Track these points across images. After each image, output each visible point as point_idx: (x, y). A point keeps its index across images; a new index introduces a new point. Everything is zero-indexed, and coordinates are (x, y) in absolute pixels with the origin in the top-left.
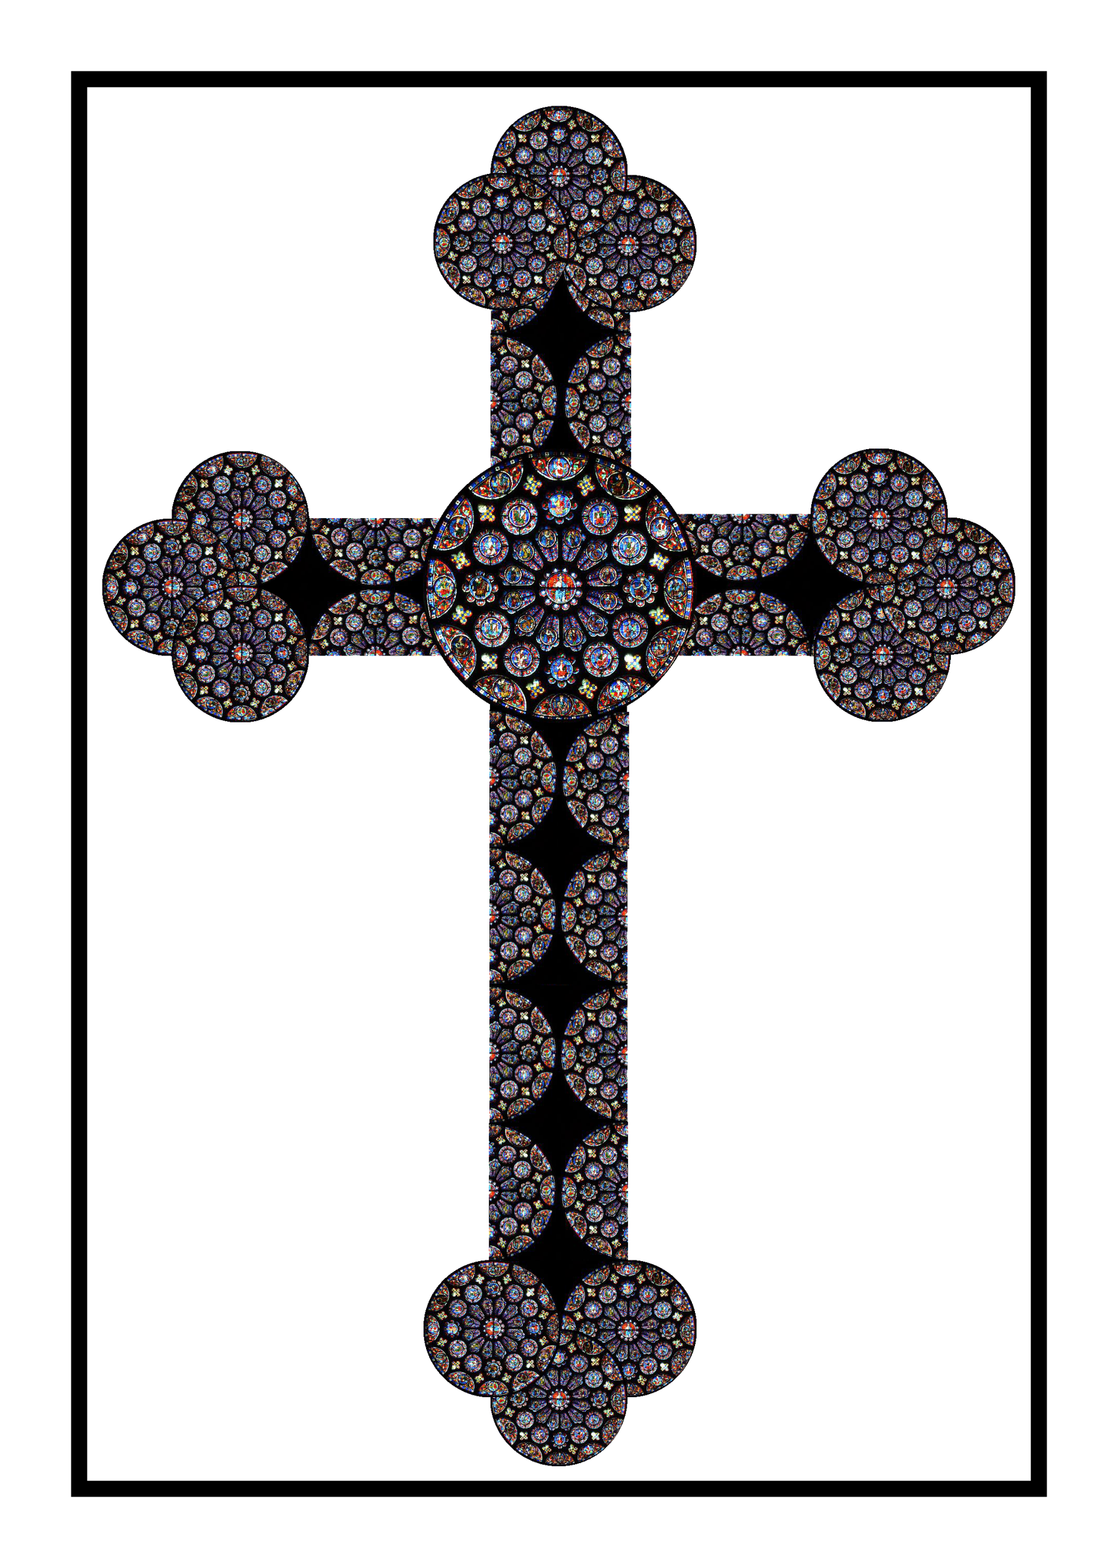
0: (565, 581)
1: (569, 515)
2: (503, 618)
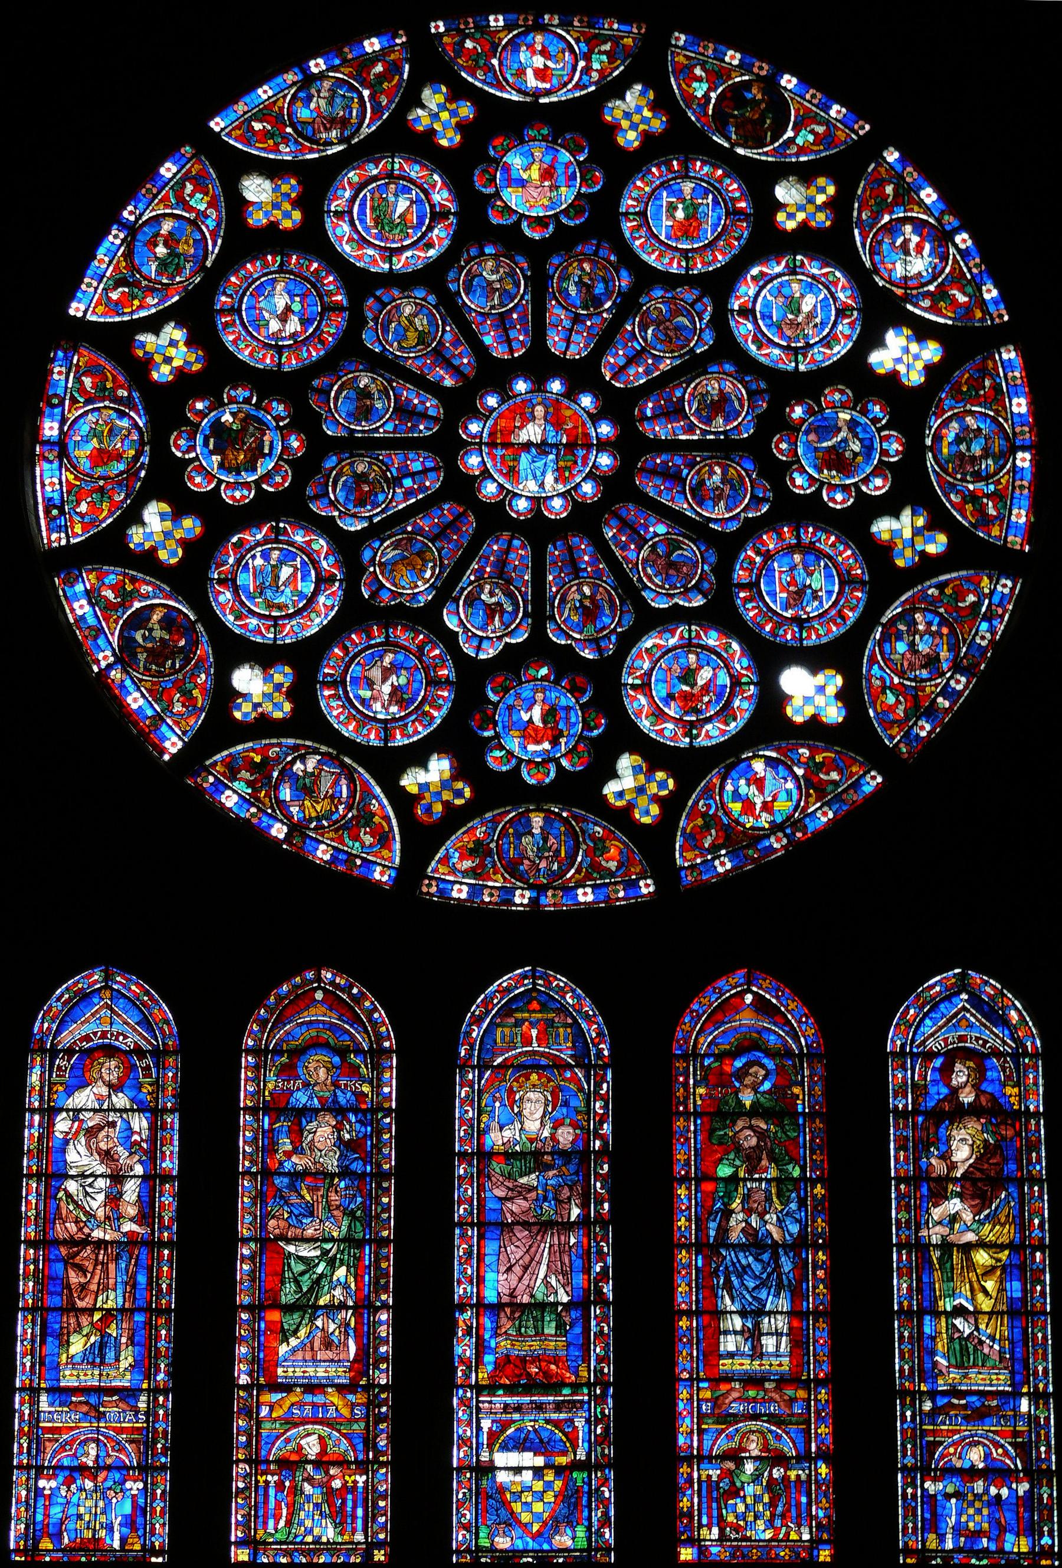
0: (555, 420)
1: (574, 208)
2: (321, 544)
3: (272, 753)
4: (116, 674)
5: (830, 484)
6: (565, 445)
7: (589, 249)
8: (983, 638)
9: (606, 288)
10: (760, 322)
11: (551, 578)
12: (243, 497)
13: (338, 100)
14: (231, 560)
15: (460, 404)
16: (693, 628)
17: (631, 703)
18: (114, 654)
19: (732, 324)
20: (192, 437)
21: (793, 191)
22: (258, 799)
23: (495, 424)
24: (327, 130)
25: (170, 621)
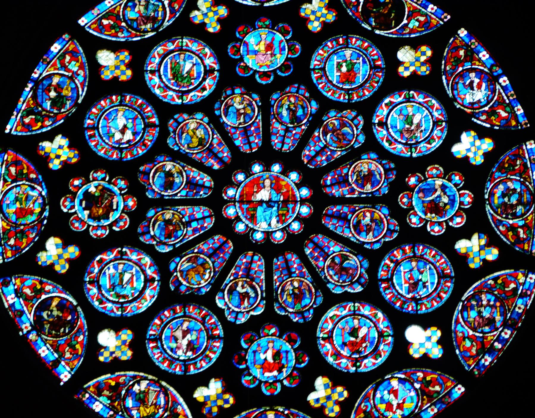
0: (276, 187)
1: (284, 67)
2: (147, 260)
3: (121, 380)
4: (33, 336)
5: (431, 221)
6: (282, 202)
7: (294, 90)
8: (519, 308)
9: (304, 112)
10: (390, 130)
11: (275, 277)
12: (102, 235)
13: (151, 7)
14: (96, 270)
15: (223, 179)
16: (357, 304)
17: (322, 348)
18: (31, 325)
19: (375, 131)
20: (73, 201)
21: (408, 54)
22: (114, 407)
23: (243, 191)
24: (145, 24)
25: (63, 305)
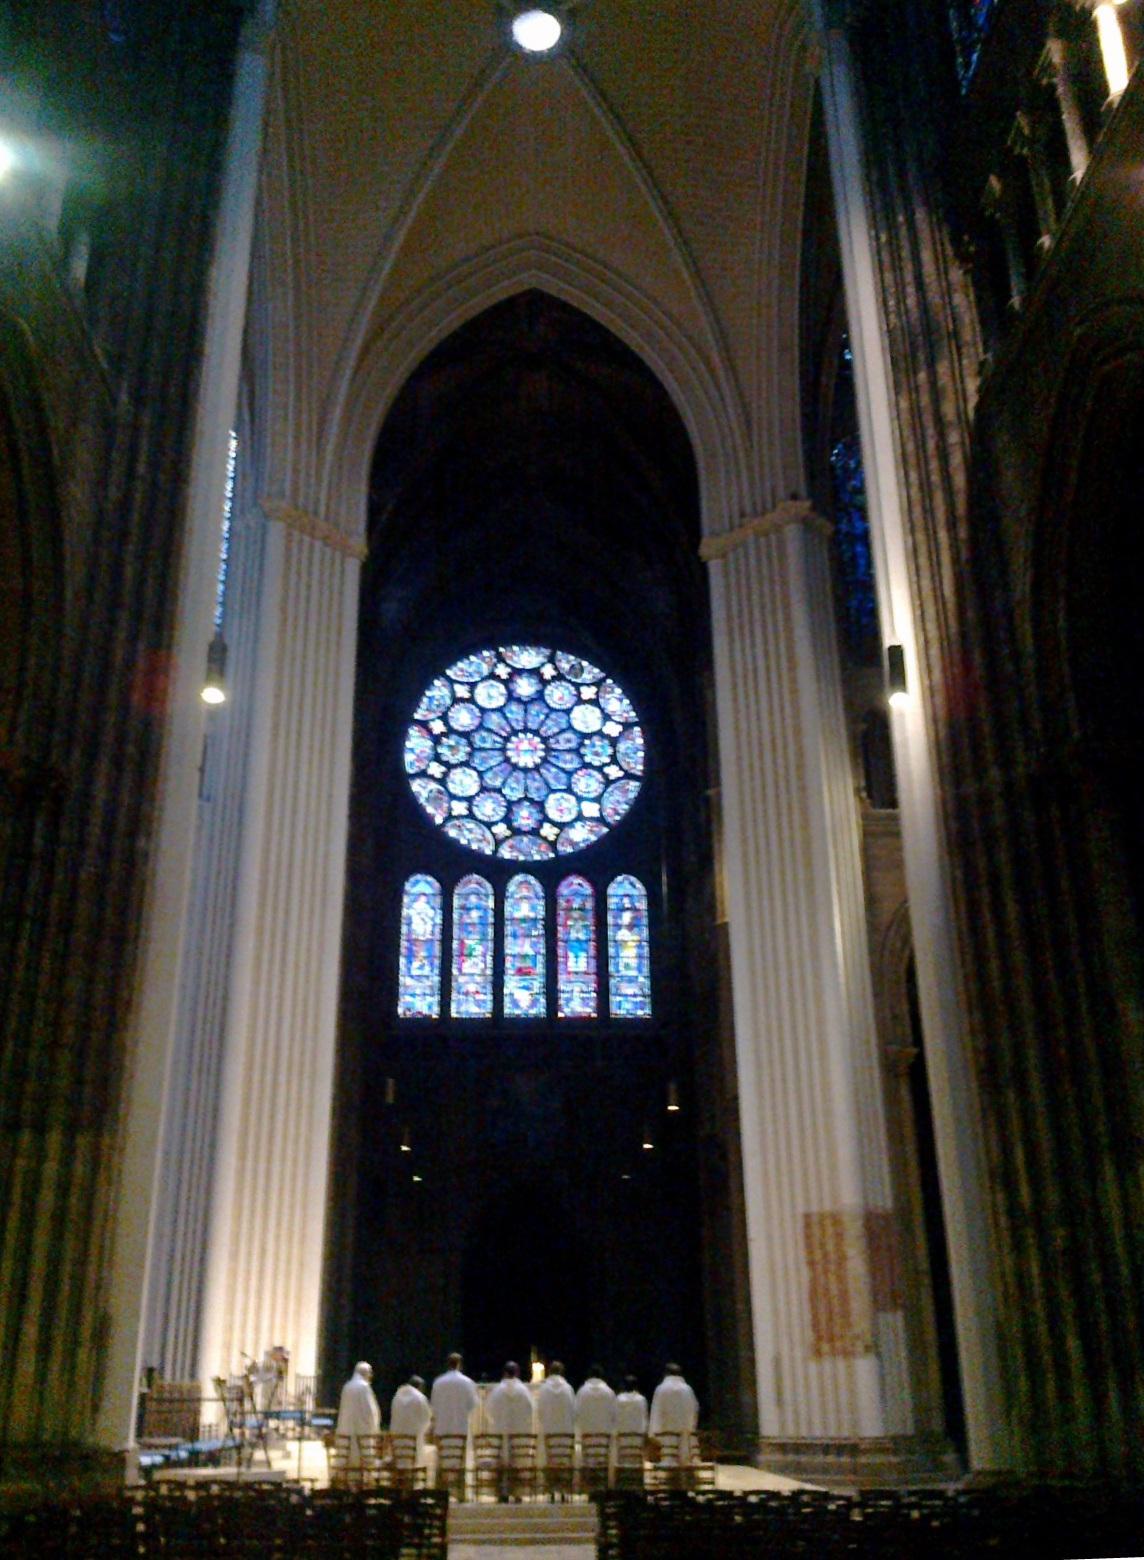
15: (507, 739)
